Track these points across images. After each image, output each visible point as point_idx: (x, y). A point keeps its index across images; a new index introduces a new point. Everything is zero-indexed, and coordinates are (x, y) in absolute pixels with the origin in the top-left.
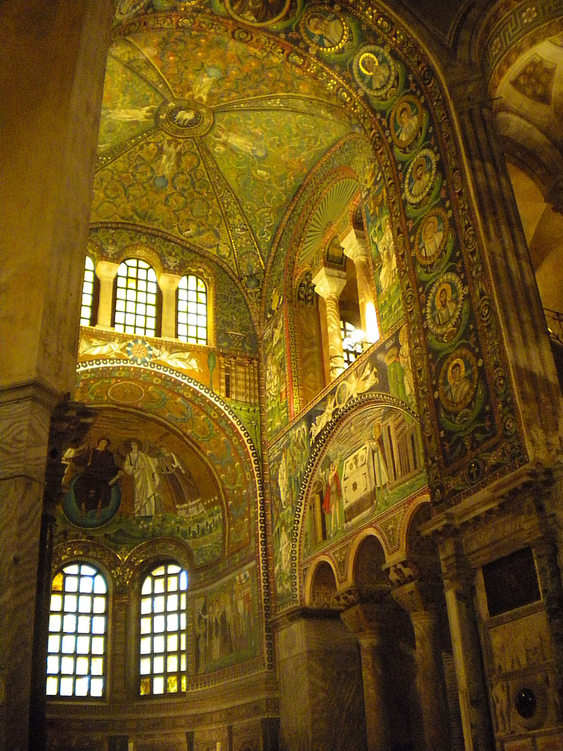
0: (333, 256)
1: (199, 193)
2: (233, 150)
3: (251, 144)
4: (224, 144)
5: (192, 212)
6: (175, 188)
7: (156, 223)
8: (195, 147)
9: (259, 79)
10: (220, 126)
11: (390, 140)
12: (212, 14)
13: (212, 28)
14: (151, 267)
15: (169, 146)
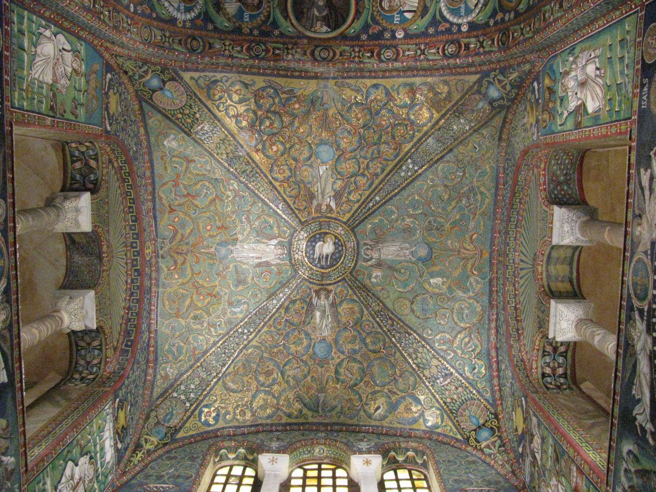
0: (560, 292)
1: (374, 352)
2: (390, 268)
3: (408, 245)
4: (379, 264)
5: (373, 382)
6: (343, 353)
7: (334, 413)
8: (351, 292)
9: (376, 137)
10: (365, 244)
11: (512, 15)
12: (282, 35)
13: (288, 53)
14: (338, 467)
15: (319, 298)
